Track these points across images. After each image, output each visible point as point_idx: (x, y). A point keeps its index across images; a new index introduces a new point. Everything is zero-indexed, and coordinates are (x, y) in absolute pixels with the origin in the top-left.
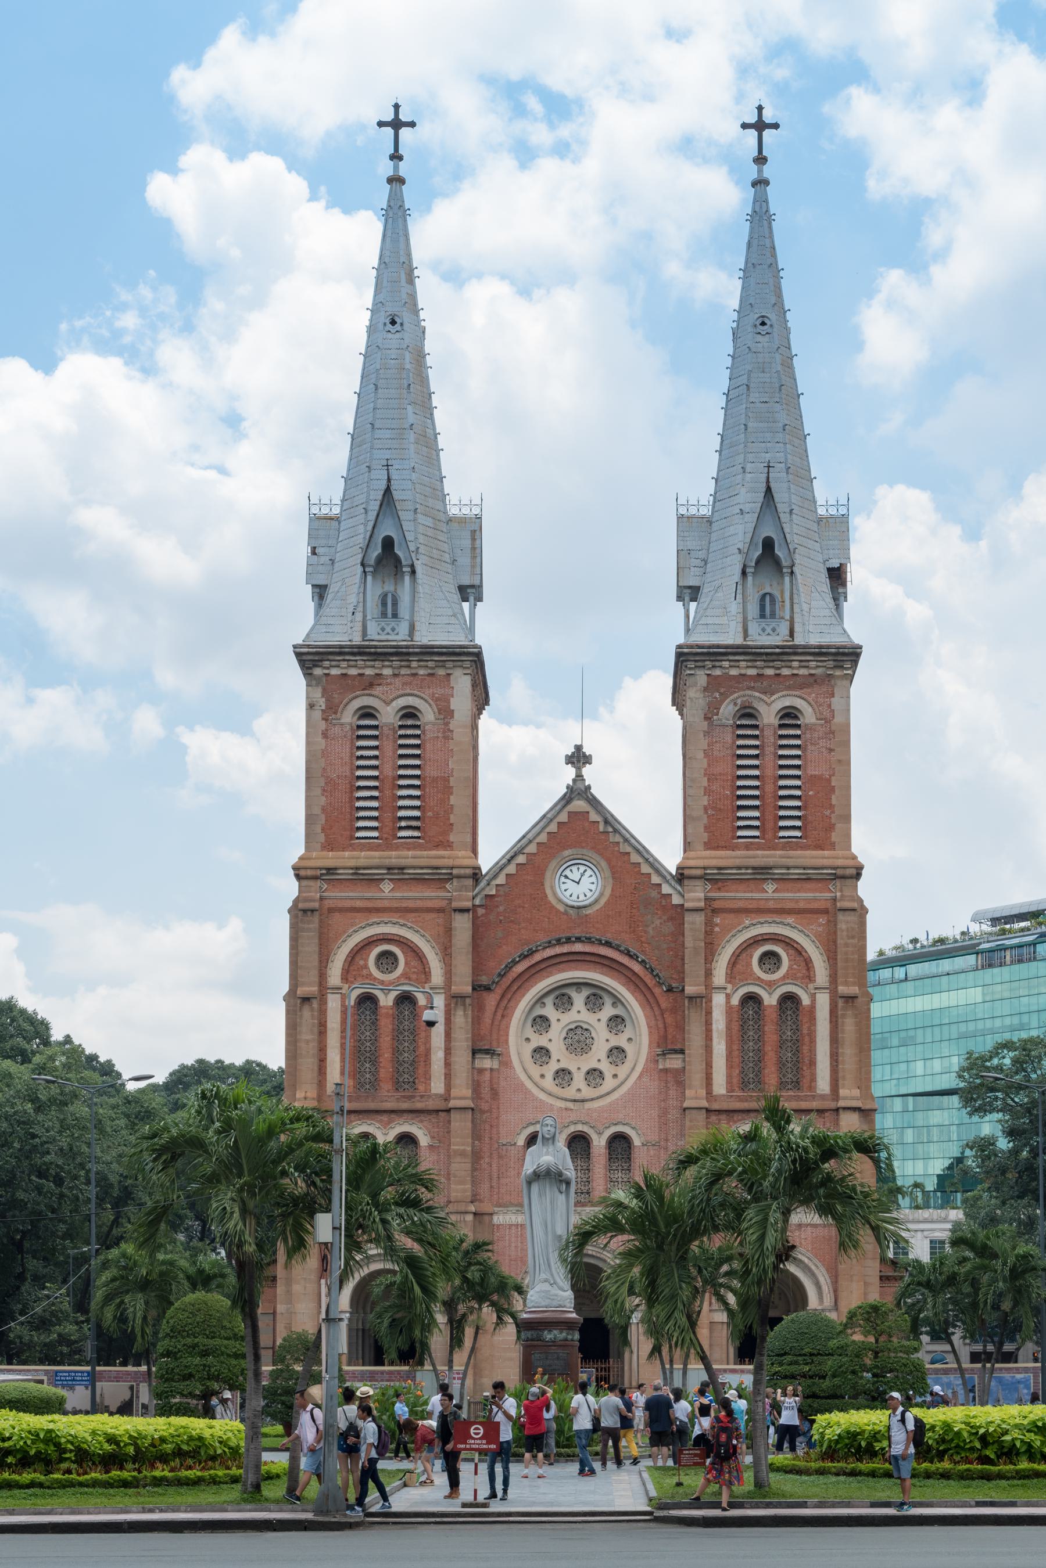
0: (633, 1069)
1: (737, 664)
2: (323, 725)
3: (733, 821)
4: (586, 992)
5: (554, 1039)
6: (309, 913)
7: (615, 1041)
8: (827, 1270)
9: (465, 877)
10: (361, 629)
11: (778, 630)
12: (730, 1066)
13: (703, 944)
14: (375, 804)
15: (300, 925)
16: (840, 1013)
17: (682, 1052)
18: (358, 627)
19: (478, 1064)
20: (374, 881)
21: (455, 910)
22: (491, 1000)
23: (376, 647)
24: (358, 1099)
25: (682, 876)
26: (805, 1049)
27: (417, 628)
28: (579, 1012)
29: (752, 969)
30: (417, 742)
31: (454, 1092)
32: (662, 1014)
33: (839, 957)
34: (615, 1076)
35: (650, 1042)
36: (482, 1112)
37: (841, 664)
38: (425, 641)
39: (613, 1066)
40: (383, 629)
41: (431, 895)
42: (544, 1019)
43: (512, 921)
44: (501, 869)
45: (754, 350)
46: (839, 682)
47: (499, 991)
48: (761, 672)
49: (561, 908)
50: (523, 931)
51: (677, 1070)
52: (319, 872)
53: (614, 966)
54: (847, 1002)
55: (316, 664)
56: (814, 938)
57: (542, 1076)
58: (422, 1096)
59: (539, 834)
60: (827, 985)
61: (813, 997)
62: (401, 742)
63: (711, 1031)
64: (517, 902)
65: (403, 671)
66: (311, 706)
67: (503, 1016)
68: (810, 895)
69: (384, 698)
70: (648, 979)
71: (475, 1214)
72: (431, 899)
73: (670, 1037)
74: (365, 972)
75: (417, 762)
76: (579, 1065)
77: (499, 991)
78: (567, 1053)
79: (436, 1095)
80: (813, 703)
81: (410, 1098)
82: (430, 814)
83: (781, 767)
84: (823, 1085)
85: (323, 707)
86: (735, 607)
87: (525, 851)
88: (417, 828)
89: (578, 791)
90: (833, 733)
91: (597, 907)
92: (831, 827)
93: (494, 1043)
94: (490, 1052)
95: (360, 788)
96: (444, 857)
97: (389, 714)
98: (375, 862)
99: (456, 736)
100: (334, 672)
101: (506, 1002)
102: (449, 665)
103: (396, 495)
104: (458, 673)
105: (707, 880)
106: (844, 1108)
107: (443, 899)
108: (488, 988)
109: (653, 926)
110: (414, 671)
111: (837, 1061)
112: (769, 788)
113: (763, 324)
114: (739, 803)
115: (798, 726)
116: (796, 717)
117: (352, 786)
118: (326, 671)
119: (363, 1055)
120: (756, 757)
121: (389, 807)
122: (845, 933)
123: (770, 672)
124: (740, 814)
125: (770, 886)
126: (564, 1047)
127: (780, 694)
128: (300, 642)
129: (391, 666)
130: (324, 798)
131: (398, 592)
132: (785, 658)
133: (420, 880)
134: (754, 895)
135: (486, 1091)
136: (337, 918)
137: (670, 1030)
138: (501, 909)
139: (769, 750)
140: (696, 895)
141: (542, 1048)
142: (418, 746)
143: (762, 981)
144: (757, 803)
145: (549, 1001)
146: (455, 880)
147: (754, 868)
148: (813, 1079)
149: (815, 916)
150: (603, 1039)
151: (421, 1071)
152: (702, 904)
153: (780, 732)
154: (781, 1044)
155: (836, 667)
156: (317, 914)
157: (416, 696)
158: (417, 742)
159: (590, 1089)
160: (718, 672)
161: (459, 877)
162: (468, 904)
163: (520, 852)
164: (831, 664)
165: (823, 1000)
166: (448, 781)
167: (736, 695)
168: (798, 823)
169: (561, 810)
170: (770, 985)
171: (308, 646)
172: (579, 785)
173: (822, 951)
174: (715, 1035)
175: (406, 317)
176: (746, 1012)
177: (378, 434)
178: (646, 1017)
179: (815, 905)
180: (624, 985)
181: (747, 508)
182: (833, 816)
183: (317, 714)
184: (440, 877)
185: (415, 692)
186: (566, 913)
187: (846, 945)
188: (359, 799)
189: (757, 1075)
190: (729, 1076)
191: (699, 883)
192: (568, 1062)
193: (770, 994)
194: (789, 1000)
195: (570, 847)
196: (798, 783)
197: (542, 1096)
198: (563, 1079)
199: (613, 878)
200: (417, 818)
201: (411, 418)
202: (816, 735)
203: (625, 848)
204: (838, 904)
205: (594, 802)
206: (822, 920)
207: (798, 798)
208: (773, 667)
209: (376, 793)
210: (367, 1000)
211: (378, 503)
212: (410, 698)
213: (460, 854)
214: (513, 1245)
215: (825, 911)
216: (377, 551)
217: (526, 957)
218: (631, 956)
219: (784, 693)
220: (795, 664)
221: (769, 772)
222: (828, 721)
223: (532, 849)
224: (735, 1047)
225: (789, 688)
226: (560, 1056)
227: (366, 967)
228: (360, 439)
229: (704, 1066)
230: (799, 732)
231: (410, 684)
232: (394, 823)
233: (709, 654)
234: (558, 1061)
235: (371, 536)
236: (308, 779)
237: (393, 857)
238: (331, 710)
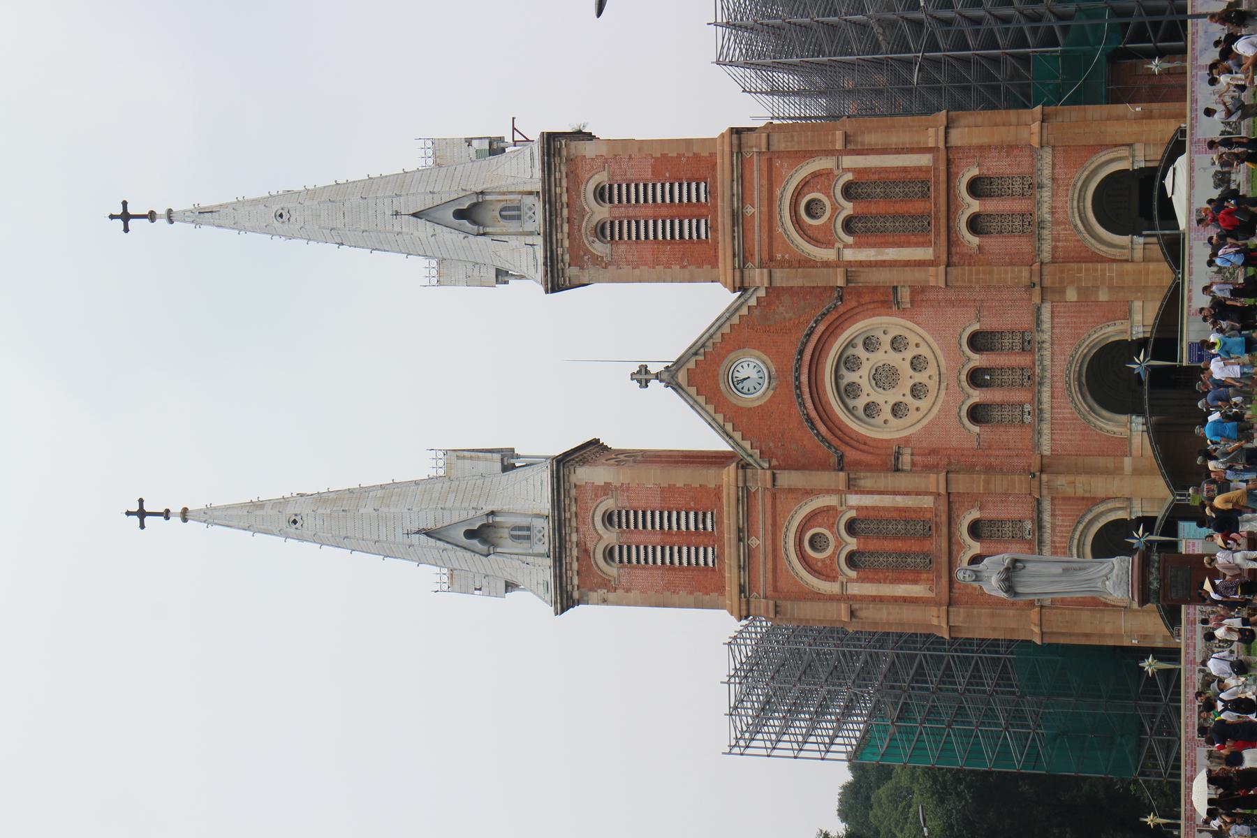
0: (911, 330)
1: (559, 241)
2: (620, 592)
3: (693, 243)
4: (843, 371)
5: (885, 398)
6: (778, 609)
7: (888, 347)
8: (1095, 153)
9: (745, 476)
10: (540, 559)
11: (531, 205)
12: (908, 244)
13: (800, 270)
14: (685, 550)
15: (788, 616)
16: (860, 148)
17: (895, 288)
18: (539, 560)
19: (907, 467)
20: (750, 553)
22: (851, 454)
23: (554, 547)
24: (938, 571)
25: (741, 287)
26: (892, 176)
27: (538, 512)
28: (861, 377)
29: (823, 225)
30: (632, 513)
31: (933, 489)
33: (810, 149)
34: (917, 345)
35: (887, 315)
36: (950, 463)
37: (557, 150)
38: (549, 506)
39: (908, 347)
40: (540, 540)
41: (761, 506)
42: (868, 407)
43: (782, 436)
44: (738, 444)
45: (302, 225)
46: (573, 151)
47: (843, 448)
48: (565, 220)
49: (770, 393)
50: (791, 426)
51: (912, 292)
52: (743, 600)
53: (820, 347)
54: (850, 142)
55: (570, 597)
56: (794, 170)
57: (918, 409)
58: (936, 515)
59: (706, 411)
60: (834, 158)
62: (632, 527)
63: (876, 261)
65: (574, 524)
66: (605, 601)
67: (865, 444)
68: (756, 175)
70: (831, 317)
71: (1042, 471)
72: (764, 505)
73: (882, 298)
74: (828, 562)
75: (649, 513)
76: (908, 377)
77: (843, 448)
78: (897, 387)
79: (934, 503)
80: (590, 174)
82: (692, 504)
83: (646, 200)
84: (924, 160)
85: (606, 591)
86: (514, 242)
87: (722, 423)
88: (705, 515)
89: (670, 376)
90: (616, 156)
91: (769, 362)
92: (696, 156)
93: (889, 452)
94: (898, 455)
95: (672, 562)
96: (729, 494)
97: (610, 537)
98: (734, 551)
99: (626, 482)
100: (576, 581)
101: (852, 441)
102: (567, 485)
103: (430, 525)
104: (573, 478)
105: (743, 267)
106: (946, 142)
107: (764, 495)
108: (841, 458)
109: (784, 312)
110: (574, 516)
111: (903, 149)
112: (664, 211)
113: (281, 216)
114: (677, 237)
116: (603, 188)
117: (670, 568)
118: (576, 588)
119: (899, 564)
120: (637, 223)
121: (687, 538)
122: (789, 144)
123: (565, 212)
124: (687, 237)
125: (748, 210)
126: (892, 390)
127: (584, 204)
128: (553, 608)
129: (570, 535)
130: (681, 592)
131: (508, 526)
132: (553, 199)
134: (756, 223)
135: (931, 460)
136: (781, 584)
137: (876, 298)
138: (771, 445)
139: (631, 212)
140: (758, 276)
141: (893, 410)
142: (636, 513)
143: (831, 216)
144: (677, 222)
145: (851, 403)
146: (748, 484)
147: (733, 226)
148: (920, 169)
149: (774, 169)
150: (884, 356)
151: (913, 515)
152: (765, 271)
153: (616, 202)
154: (886, 196)
155: (560, 155)
156: (778, 602)
157: (594, 514)
158: (632, 513)
159: (929, 367)
160: (567, 257)
161: (745, 481)
162: (768, 473)
163: (723, 428)
165: (849, 161)
166: (665, 487)
167: (585, 241)
168: (694, 185)
169: (687, 393)
170: (836, 208)
171: (556, 603)
172: (665, 376)
173: (805, 163)
174: (880, 258)
175: (290, 511)
176: (860, 229)
177: (383, 537)
178: (863, 320)
179: (765, 169)
180: (837, 338)
181: (430, 231)
182: (686, 155)
183: (611, 596)
184: (746, 497)
185: (591, 514)
186: (775, 389)
187: (799, 142)
188: (681, 563)
189: (916, 219)
190: (918, 245)
191: (746, 272)
193: (843, 209)
194: (848, 191)
195: (718, 385)
196: (659, 186)
197: (935, 410)
198: (920, 391)
199: (744, 348)
201: (369, 510)
202: (618, 171)
203: (718, 339)
204: (764, 150)
205: (680, 363)
206: (778, 163)
207: (672, 186)
208: (561, 209)
209: (676, 549)
210: (852, 560)
211: (438, 542)
212: (596, 519)
213: (725, 479)
214: (1070, 437)
215: (770, 161)
216: (475, 543)
217: (813, 424)
219: (583, 200)
220: (558, 190)
221: (650, 212)
222: (606, 161)
223: (720, 418)
224: (891, 240)
225: (579, 196)
226: (900, 393)
227: (823, 561)
228: (388, 551)
229: (907, 268)
230: (616, 186)
231: (584, 518)
232: (700, 534)
233: (552, 266)
234: (904, 395)
235: (465, 548)
236: (664, 606)
237: (730, 535)
238: (606, 584)
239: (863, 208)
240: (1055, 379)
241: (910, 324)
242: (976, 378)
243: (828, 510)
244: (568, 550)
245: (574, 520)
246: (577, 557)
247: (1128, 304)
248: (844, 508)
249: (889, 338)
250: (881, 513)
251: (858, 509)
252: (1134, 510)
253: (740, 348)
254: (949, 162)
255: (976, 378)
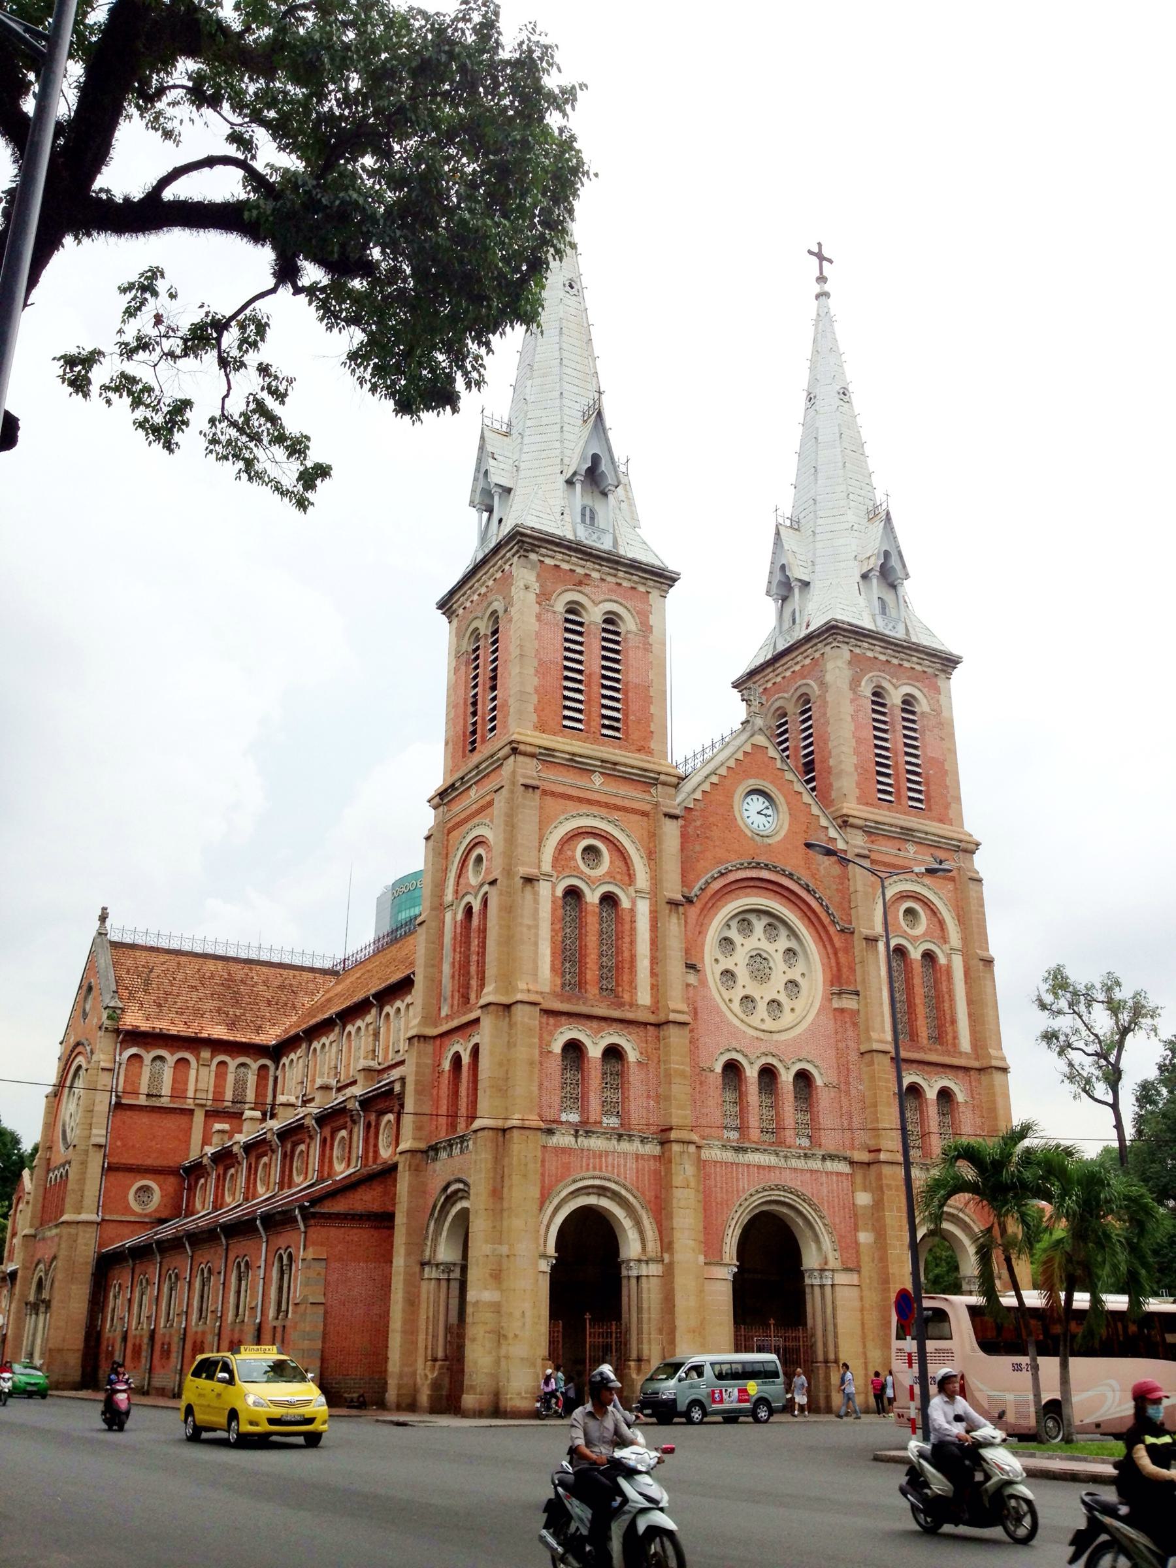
2: (537, 608)
4: (765, 920)
5: (739, 961)
17: (857, 994)
20: (586, 771)
21: (666, 815)
26: (947, 1005)
32: (836, 954)
34: (792, 1010)
38: (630, 556)
42: (727, 942)
47: (698, 905)
49: (750, 834)
52: (538, 751)
53: (793, 898)
61: (949, 956)
64: (711, 819)
65: (609, 579)
69: (593, 596)
70: (823, 916)
72: (638, 800)
74: (572, 864)
81: (621, 1005)
88: (617, 729)
92: (947, 806)
97: (594, 615)
99: (654, 649)
102: (651, 583)
108: (689, 901)
110: (619, 581)
115: (913, 713)
123: (895, 661)
133: (627, 779)
138: (698, 823)
147: (902, 828)
151: (626, 978)
157: (621, 604)
161: (664, 784)
164: (939, 666)
191: (860, 832)
192: (753, 990)
200: (617, 720)
210: (573, 894)
212: (615, 605)
214: (719, 1185)
217: (722, 874)
218: (809, 891)
220: (914, 659)
222: (939, 714)
223: (723, 771)
225: (909, 678)
227: (573, 858)
239: (917, 968)
240: (777, 1172)
241: (817, 1005)
242: (768, 1074)
243: (629, 875)
244: (583, 563)
245: (613, 580)
246: (572, 571)
247: (856, 1270)
248: (634, 895)
249: (799, 979)
250: (627, 940)
251: (632, 910)
252: (644, 1266)
253: (790, 809)
254: (966, 1069)
255: (768, 1074)
